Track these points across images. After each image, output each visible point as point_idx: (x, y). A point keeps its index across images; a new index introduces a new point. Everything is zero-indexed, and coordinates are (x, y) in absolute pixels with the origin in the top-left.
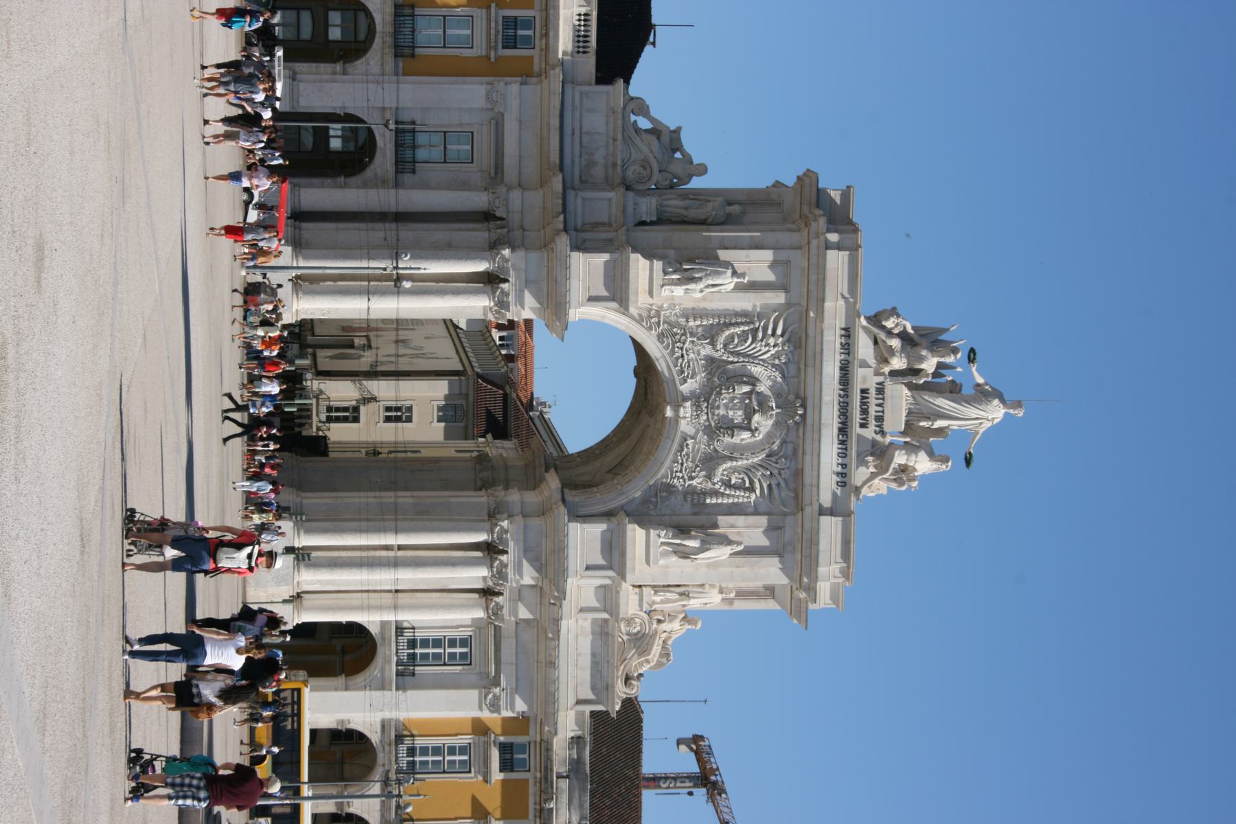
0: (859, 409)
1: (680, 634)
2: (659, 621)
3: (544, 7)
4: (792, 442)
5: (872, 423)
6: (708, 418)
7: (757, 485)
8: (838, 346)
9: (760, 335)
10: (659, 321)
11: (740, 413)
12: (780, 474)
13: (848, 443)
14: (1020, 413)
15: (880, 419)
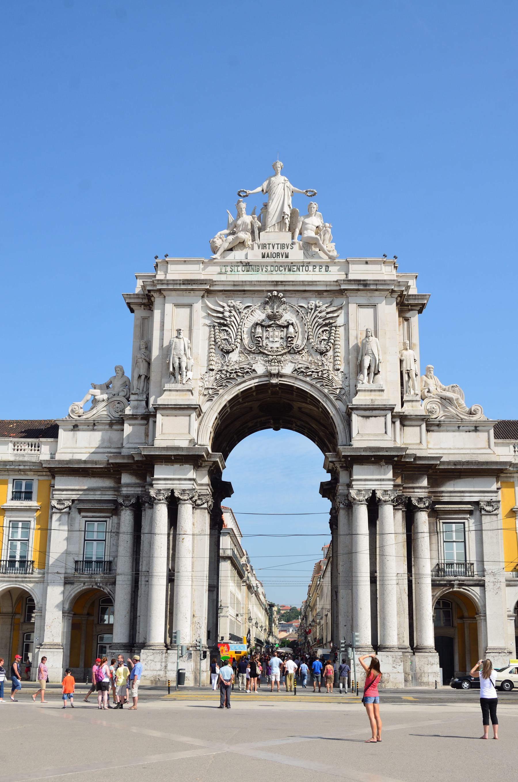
0: (276, 258)
1: (438, 380)
2: (429, 392)
3: (6, 473)
4: (298, 301)
5: (286, 250)
6: (280, 355)
7: (327, 321)
8: (233, 273)
9: (222, 321)
10: (212, 389)
11: (276, 333)
12: (319, 307)
13: (298, 265)
14: (280, 164)
15: (283, 246)
